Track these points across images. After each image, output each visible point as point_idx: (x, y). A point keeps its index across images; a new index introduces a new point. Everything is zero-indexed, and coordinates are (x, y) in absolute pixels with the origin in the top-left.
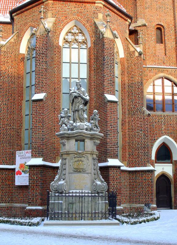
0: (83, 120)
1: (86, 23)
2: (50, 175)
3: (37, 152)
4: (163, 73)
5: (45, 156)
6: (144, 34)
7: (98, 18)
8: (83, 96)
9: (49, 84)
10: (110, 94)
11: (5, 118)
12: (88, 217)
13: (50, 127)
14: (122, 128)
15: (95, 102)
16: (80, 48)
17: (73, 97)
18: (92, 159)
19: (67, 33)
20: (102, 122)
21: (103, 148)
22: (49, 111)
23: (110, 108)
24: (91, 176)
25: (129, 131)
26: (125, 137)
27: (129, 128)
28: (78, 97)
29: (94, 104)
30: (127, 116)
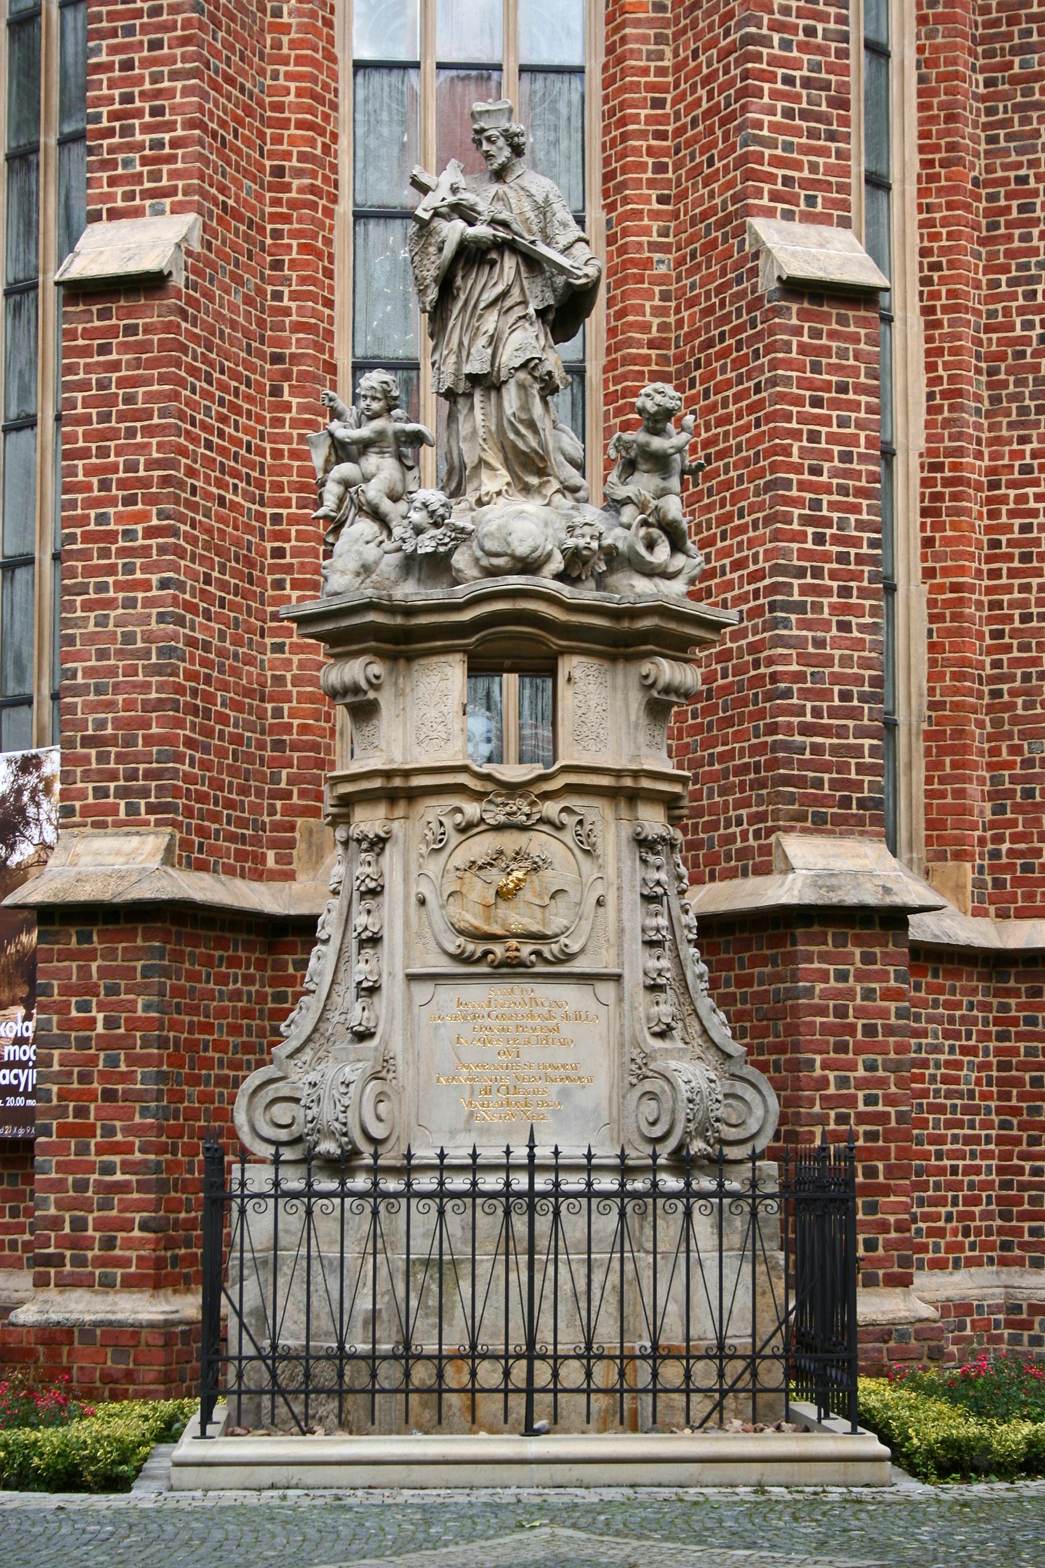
0: (542, 472)
2: (237, 995)
3: (113, 776)
5: (189, 812)
8: (542, 248)
9: (223, 124)
10: (809, 218)
12: (588, 1392)
13: (237, 542)
14: (928, 542)
15: (665, 296)
17: (449, 250)
20: (727, 485)
21: (738, 737)
22: (223, 387)
23: (803, 349)
24: (620, 1000)
25: (995, 574)
26: (960, 632)
27: (995, 544)
28: (494, 255)
29: (657, 312)
30: (978, 427)
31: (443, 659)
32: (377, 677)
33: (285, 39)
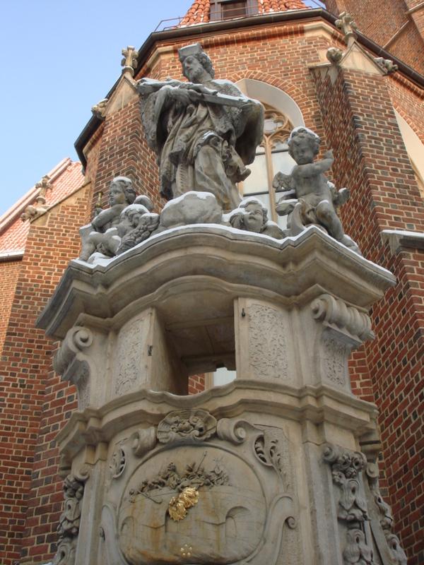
1: (280, 78)
3: (47, 529)
11: (12, 435)
16: (273, 152)
18: (317, 473)
31: (136, 318)
32: (85, 341)
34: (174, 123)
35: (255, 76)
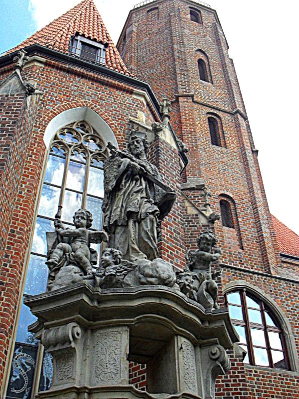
1: (110, 118)
4: (244, 280)
6: (200, 202)
7: (136, 118)
19: (64, 129)
28: (138, 177)
32: (78, 334)
33: (22, 199)
34: (125, 183)
35: (95, 108)
